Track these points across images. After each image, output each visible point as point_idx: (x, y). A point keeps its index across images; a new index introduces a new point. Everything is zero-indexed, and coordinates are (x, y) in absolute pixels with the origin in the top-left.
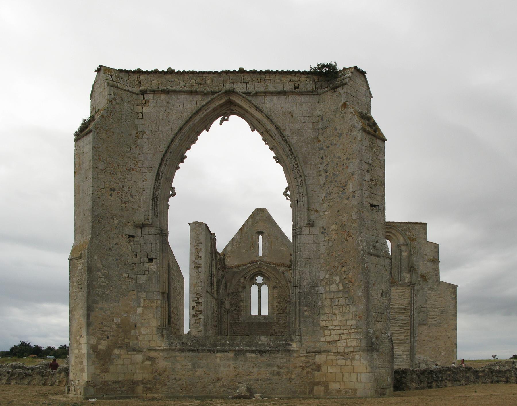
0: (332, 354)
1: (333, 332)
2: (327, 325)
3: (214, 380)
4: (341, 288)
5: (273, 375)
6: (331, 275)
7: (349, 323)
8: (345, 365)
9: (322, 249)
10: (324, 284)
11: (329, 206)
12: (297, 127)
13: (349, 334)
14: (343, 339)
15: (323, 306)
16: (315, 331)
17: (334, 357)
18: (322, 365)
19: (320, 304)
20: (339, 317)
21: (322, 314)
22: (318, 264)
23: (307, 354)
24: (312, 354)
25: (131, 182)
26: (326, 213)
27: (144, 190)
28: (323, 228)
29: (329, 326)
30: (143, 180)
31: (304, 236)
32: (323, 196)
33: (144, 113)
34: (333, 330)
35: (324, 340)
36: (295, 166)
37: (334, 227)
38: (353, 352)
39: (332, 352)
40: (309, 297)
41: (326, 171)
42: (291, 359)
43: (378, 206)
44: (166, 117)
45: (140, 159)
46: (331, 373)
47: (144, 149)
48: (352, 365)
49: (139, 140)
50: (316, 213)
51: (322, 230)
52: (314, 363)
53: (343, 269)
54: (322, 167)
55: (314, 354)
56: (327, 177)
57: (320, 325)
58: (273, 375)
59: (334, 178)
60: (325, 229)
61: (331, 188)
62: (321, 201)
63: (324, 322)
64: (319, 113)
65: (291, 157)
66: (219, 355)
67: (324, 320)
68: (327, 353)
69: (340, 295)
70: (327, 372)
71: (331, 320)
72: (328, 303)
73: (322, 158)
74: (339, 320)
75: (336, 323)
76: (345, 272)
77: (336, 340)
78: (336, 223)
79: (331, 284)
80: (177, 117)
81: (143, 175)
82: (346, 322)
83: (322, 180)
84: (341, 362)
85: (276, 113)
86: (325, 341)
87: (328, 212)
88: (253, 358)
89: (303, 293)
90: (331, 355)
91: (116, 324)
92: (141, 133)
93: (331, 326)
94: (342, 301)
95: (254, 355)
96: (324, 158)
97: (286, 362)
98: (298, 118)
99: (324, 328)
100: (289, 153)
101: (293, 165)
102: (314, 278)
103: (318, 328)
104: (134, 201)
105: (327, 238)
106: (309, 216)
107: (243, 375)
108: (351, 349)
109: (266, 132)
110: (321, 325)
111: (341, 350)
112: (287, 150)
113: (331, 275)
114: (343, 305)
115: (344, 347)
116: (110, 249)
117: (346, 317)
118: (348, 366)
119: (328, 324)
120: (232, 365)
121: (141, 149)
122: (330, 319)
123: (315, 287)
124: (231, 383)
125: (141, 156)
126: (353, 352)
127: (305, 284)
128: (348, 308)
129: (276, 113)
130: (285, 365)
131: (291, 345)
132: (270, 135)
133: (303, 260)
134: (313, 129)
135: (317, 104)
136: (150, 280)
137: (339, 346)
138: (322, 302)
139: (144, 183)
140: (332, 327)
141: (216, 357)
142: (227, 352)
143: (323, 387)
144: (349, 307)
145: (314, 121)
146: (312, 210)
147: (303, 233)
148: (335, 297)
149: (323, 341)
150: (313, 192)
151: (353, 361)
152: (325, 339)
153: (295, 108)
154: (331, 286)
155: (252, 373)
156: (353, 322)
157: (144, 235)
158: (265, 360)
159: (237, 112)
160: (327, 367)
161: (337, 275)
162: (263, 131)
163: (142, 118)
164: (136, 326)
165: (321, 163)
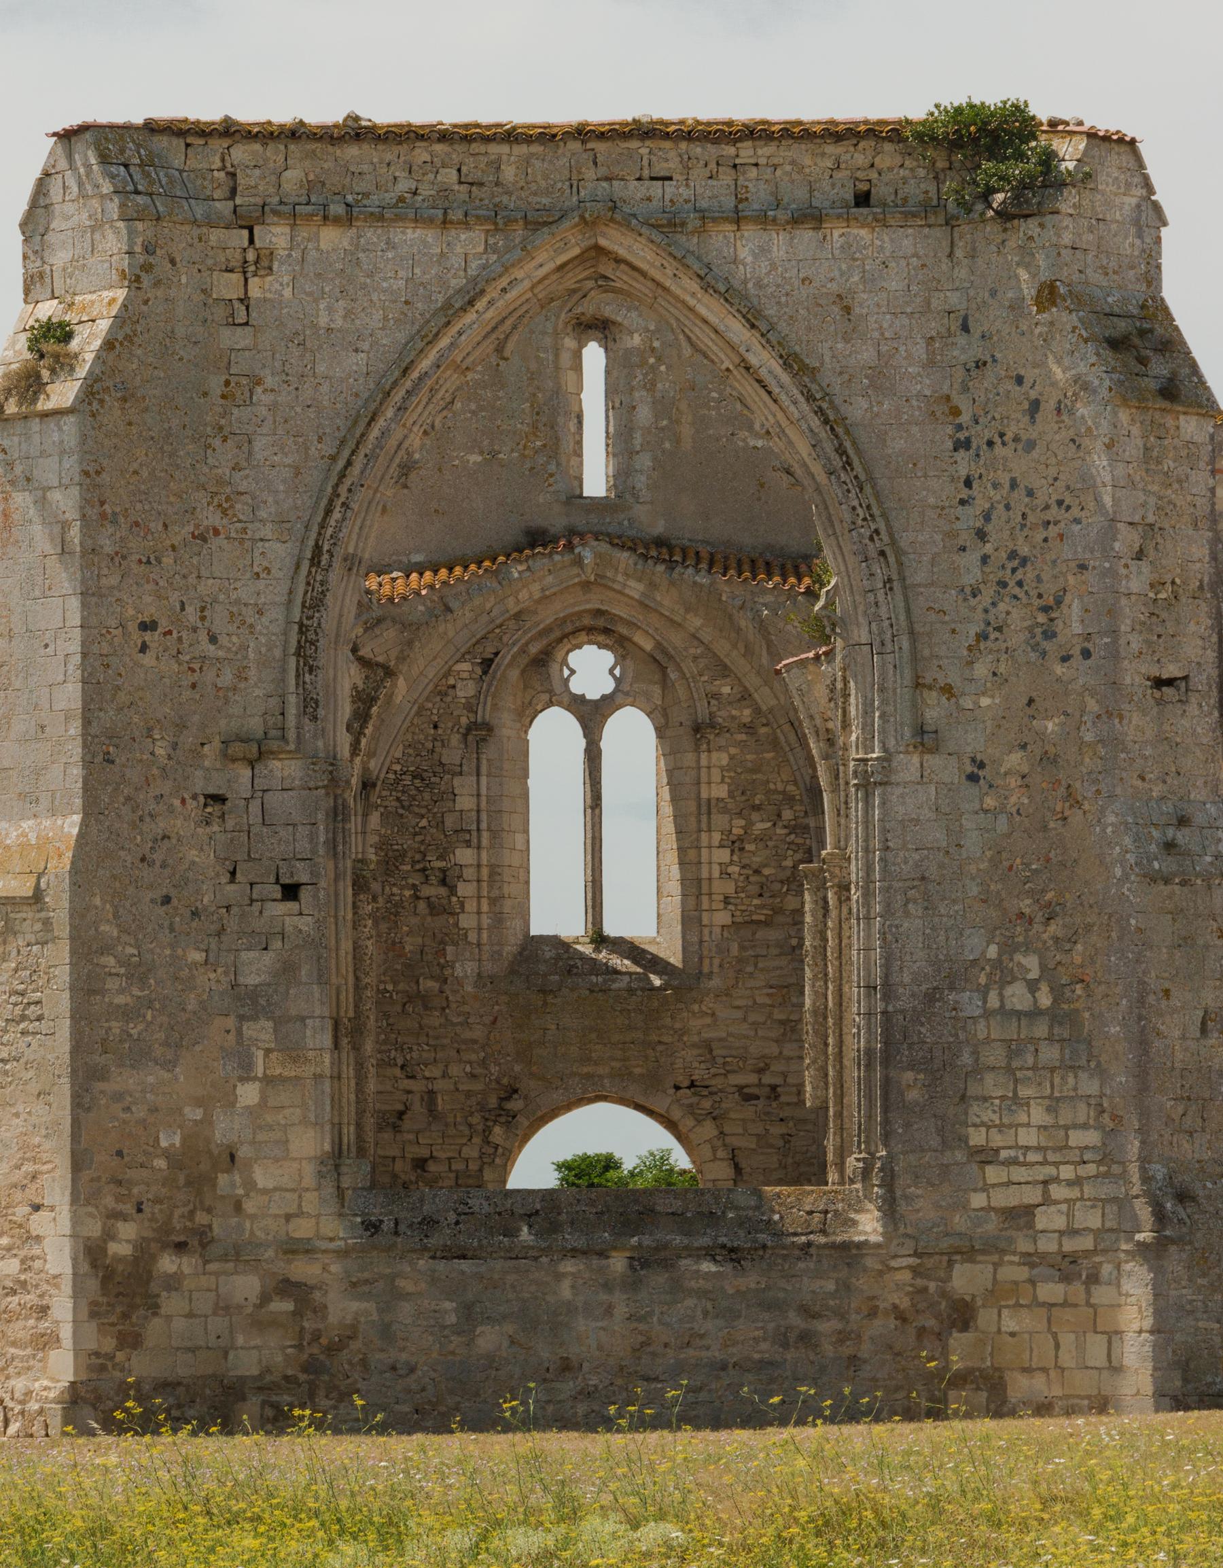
0: (1016, 1259)
1: (1019, 1174)
2: (993, 1145)
3: (548, 1369)
4: (1045, 1000)
5: (785, 1345)
6: (1009, 948)
7: (1077, 1138)
8: (1065, 1304)
9: (973, 842)
10: (983, 980)
11: (995, 674)
12: (867, 355)
13: (1077, 1182)
14: (1056, 1202)
15: (977, 1071)
16: (947, 1166)
17: (1023, 1273)
18: (979, 1303)
19: (966, 1058)
20: (1038, 1115)
21: (977, 1098)
22: (954, 901)
23: (919, 1261)
24: (937, 1257)
25: (211, 581)
26: (985, 701)
27: (260, 613)
28: (973, 760)
29: (1004, 1148)
30: (256, 569)
31: (898, 791)
32: (972, 633)
33: (252, 302)
34: (1014, 1162)
35: (985, 1204)
36: (860, 510)
37: (1015, 759)
38: (1095, 1251)
39: (1014, 1253)
40: (923, 1030)
41: (981, 535)
42: (854, 1280)
43: (1186, 678)
44: (345, 317)
45: (241, 489)
46: (1012, 1334)
47: (256, 449)
48: (1088, 1304)
49: (235, 411)
50: (944, 699)
51: (969, 768)
52: (943, 1294)
53: (1052, 928)
54: (970, 518)
55: (945, 1258)
56: (985, 559)
57: (966, 1143)
58: (785, 1345)
59: (1014, 570)
60: (982, 765)
61: (1002, 606)
62: (965, 653)
63: (983, 1130)
64: (954, 299)
65: (843, 477)
66: (568, 1266)
67: (983, 1124)
68: (995, 1258)
69: (1041, 1030)
70: (999, 1331)
71: (1010, 1126)
72: (995, 1056)
73: (968, 483)
74: (1039, 1127)
75: (1028, 1137)
76: (1056, 940)
77: (1031, 1202)
78: (1024, 747)
79: (1010, 983)
80: (385, 318)
81: (256, 553)
82: (1067, 1136)
83: (970, 569)
84: (1051, 1291)
85: (783, 299)
86: (989, 1209)
87: (993, 697)
88: (708, 1276)
89: (901, 1017)
90: (1012, 1263)
91: (167, 1154)
92: (244, 381)
93: (1010, 1148)
94: (1050, 1054)
95: (707, 1267)
96: (975, 485)
97: (837, 1291)
98: (872, 319)
99: (986, 1156)
100: (838, 462)
101: (854, 508)
102: (941, 957)
103: (960, 1156)
104: (221, 653)
105: (990, 802)
106: (916, 708)
107: (666, 1345)
108: (1087, 1243)
109: (743, 371)
110: (971, 1143)
111: (1048, 1245)
112: (829, 448)
113: (1009, 948)
114: (1052, 1070)
115: (1061, 1233)
116: (143, 859)
117: (1065, 1117)
118: (1076, 1305)
119: (997, 1140)
120: (621, 1311)
121: (245, 447)
122: (1005, 1121)
123: (946, 992)
124: (619, 1382)
125: (247, 477)
126: (1095, 1251)
127: (907, 979)
128: (1071, 1080)
129: (783, 299)
130: (831, 1303)
131: (855, 1223)
132: (759, 381)
133: (896, 885)
134: (931, 363)
135: (945, 265)
136: (288, 970)
137: (1039, 1226)
138: (975, 1053)
139: (261, 584)
140: (1012, 1153)
141: (559, 1277)
142: (602, 1254)
143: (985, 1394)
144: (1076, 1077)
145: (934, 333)
146: (930, 688)
147: (893, 778)
148: (1022, 1036)
149: (982, 1209)
150: (932, 616)
151: (1093, 1288)
152: (989, 1197)
153: (856, 278)
154: (1009, 991)
155: (702, 1336)
156: (1092, 1138)
157: (264, 791)
158: (753, 1286)
159: (625, 287)
160: (996, 1311)
161: (1028, 948)
162: (731, 367)
163: (247, 324)
164: (232, 1157)
165: (963, 502)
